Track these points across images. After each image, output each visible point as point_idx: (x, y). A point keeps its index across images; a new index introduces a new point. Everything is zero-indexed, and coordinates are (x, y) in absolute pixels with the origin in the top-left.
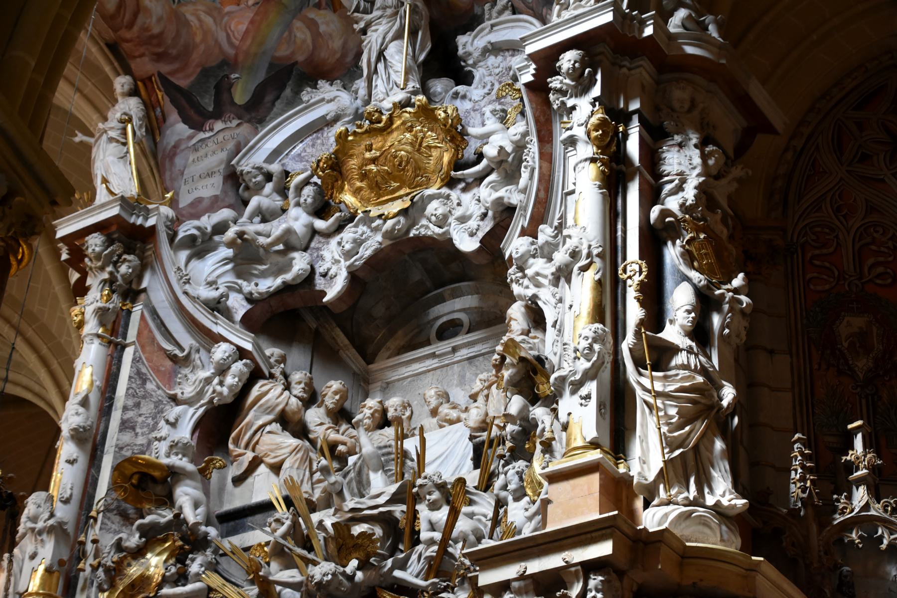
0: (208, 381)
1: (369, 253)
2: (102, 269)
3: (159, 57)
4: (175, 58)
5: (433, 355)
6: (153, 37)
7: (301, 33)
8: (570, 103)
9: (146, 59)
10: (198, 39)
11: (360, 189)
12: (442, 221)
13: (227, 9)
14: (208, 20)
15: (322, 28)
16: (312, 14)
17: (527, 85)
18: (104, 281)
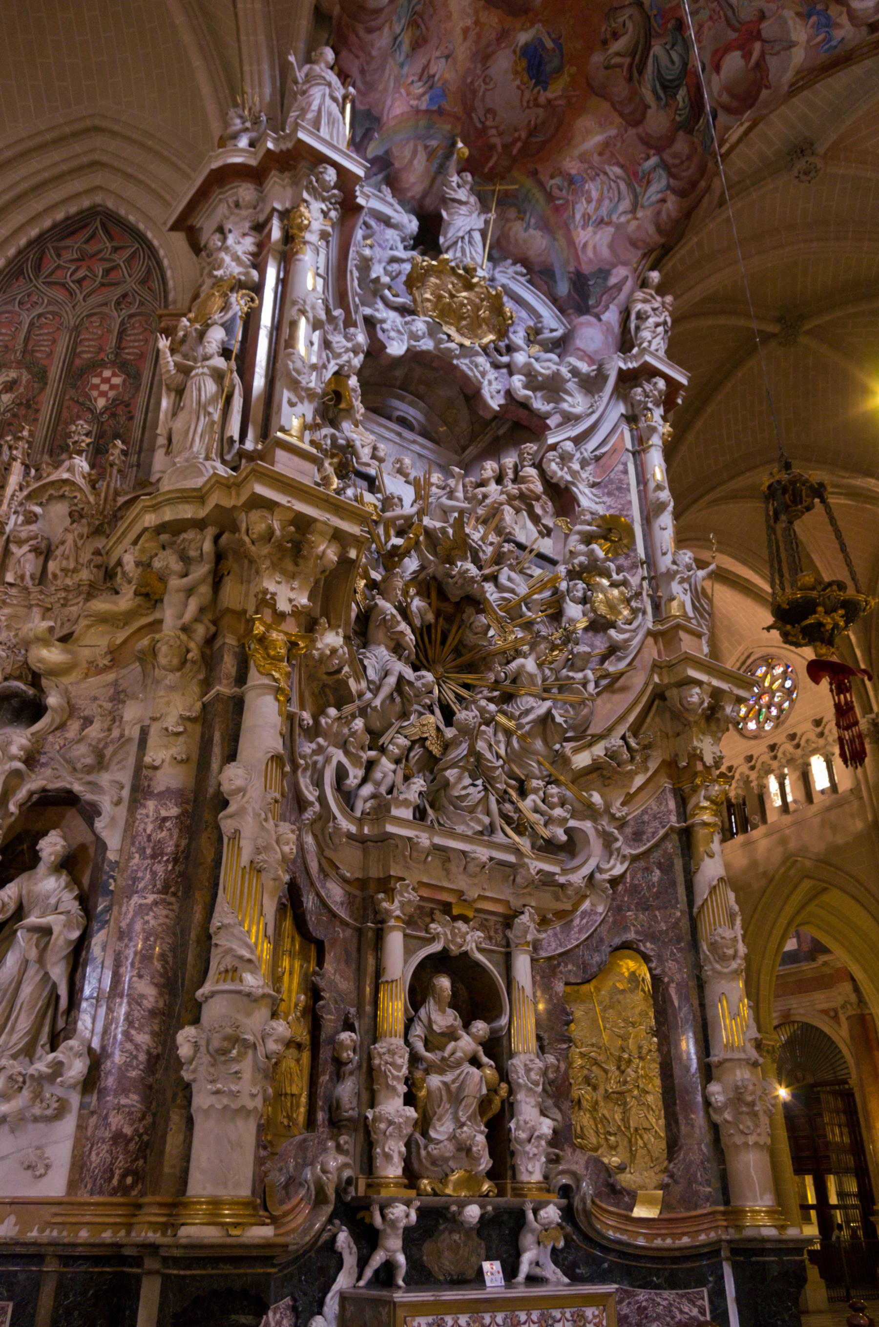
0: (347, 350)
1: (424, 348)
2: (324, 200)
3: (362, 71)
4: (365, 83)
5: (399, 434)
6: (369, 54)
7: (407, 153)
8: (650, 405)
9: (357, 63)
10: (381, 87)
11: (428, 300)
12: (483, 374)
13: (403, 91)
14: (392, 84)
15: (416, 162)
16: (420, 148)
17: (620, 369)
18: (322, 211)
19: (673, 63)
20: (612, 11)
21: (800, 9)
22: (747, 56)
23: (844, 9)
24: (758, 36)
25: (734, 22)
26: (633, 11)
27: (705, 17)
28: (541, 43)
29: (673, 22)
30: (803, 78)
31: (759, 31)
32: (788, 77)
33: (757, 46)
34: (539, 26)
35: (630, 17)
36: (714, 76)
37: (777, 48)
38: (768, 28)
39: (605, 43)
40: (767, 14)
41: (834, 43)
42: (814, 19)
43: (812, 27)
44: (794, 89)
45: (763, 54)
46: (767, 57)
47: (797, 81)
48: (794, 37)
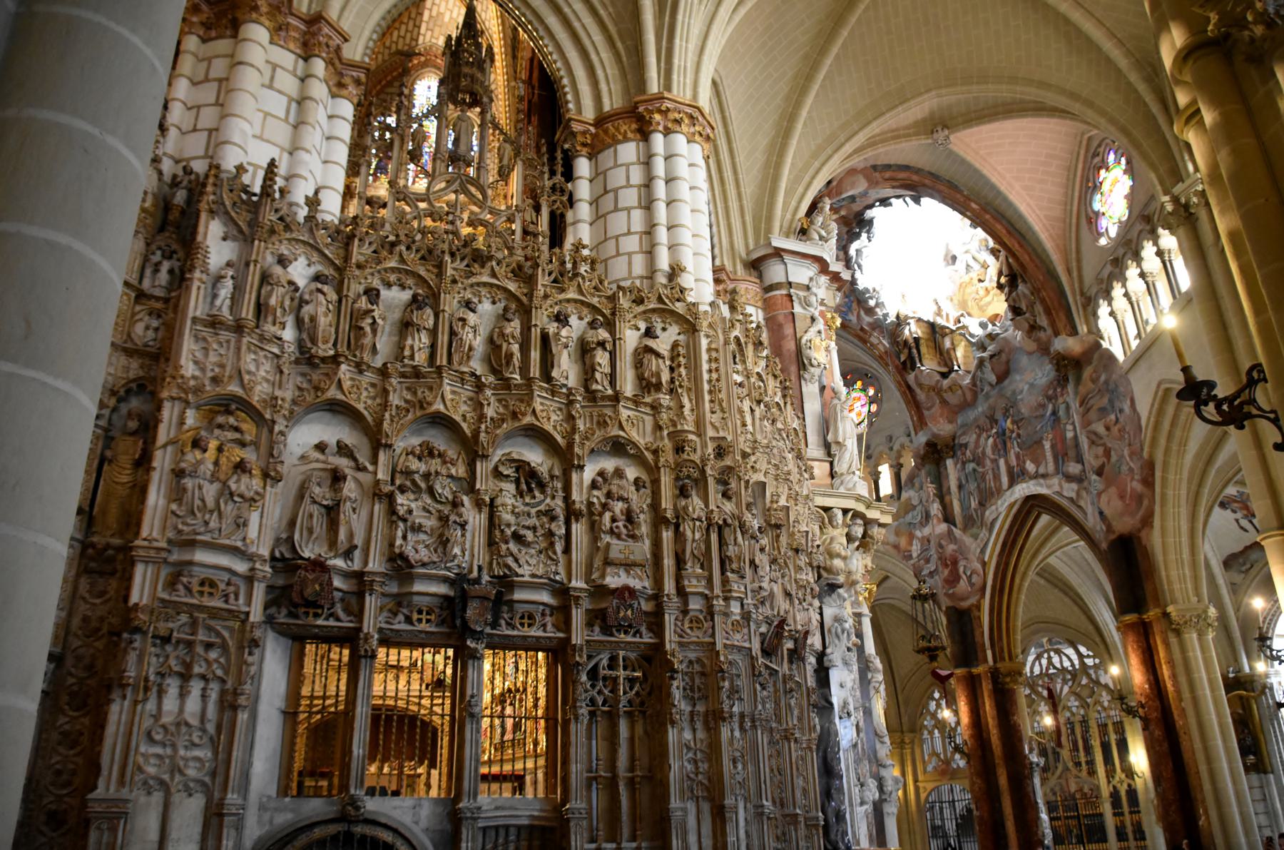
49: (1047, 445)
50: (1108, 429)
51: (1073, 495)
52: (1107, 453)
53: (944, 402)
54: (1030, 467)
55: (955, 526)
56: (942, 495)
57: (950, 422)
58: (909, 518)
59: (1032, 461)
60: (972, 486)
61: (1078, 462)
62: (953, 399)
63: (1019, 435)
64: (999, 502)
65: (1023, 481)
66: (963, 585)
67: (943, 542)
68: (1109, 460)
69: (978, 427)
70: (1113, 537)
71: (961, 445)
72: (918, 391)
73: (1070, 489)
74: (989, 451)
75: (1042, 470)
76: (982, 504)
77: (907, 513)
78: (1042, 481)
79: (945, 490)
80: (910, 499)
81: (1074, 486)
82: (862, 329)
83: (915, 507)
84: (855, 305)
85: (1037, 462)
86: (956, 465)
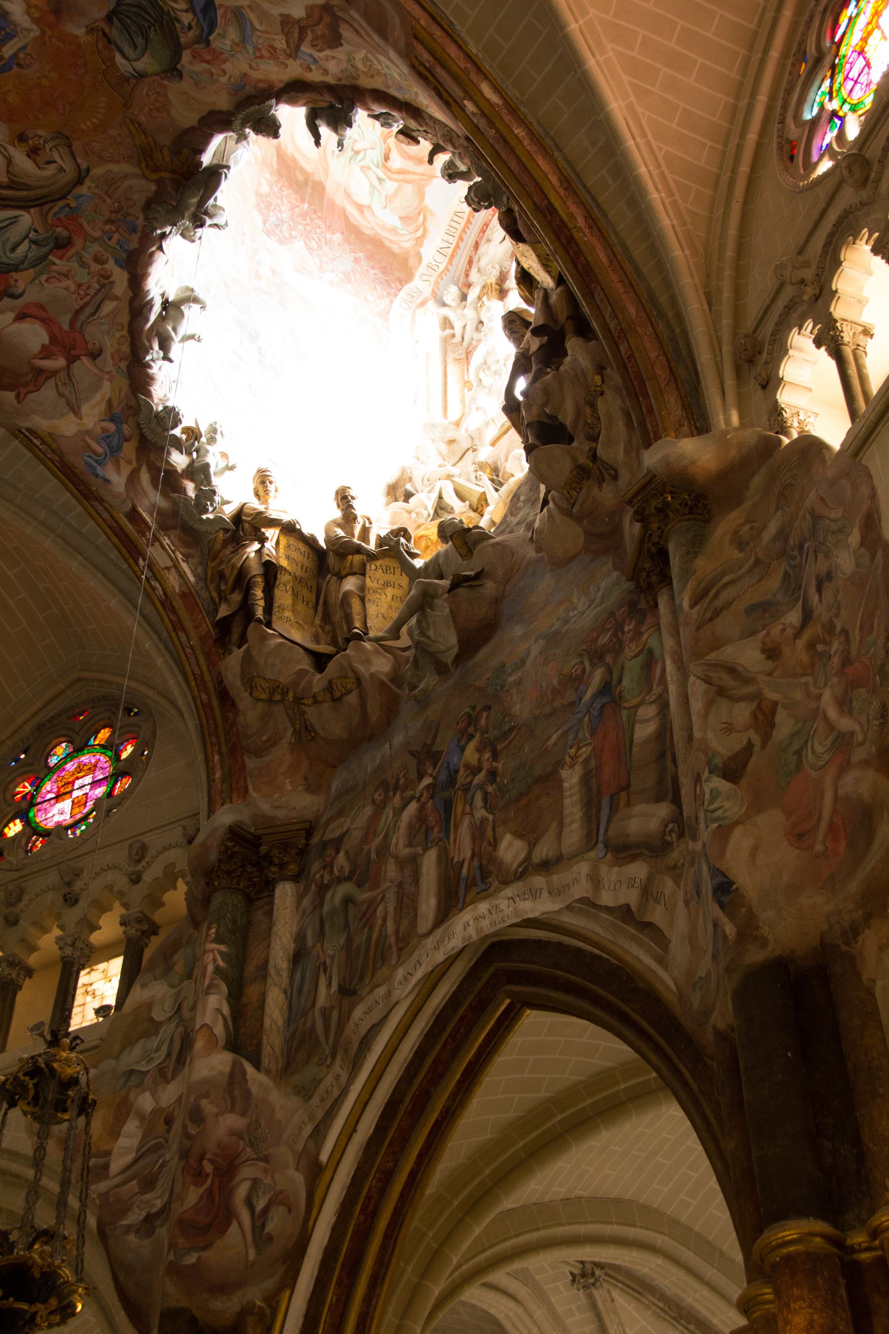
19: (13, 249)
20: (65, 139)
21: (115, 404)
22: (46, 352)
23: (135, 465)
24: (72, 359)
25: (82, 317)
26: (71, 172)
27: (78, 279)
28: (9, 37)
29: (65, 233)
30: (43, 442)
31: (78, 358)
32: (41, 423)
33: (61, 362)
34: (36, 31)
35: (62, 170)
36: (11, 316)
37: (66, 391)
38: (83, 367)
39: (22, 138)
40: (99, 360)
41: (100, 471)
42: (111, 427)
43: (104, 430)
44: (28, 437)
45: (54, 373)
46: (50, 384)
47: (38, 437)
48: (85, 409)
49: (571, 778)
50: (772, 653)
51: (632, 897)
52: (765, 718)
53: (305, 733)
54: (511, 850)
55: (257, 1065)
56: (240, 982)
57: (313, 788)
58: (132, 1058)
59: (518, 835)
60: (332, 948)
61: (659, 799)
62: (331, 723)
63: (493, 775)
64: (400, 973)
65: (485, 894)
66: (235, 1243)
67: (207, 1106)
68: (766, 737)
69: (384, 785)
70: (755, 956)
71: (324, 845)
72: (244, 700)
73: (621, 884)
74: (399, 842)
75: (543, 851)
76: (348, 992)
77: (128, 1043)
78: (538, 881)
79: (251, 967)
80: (149, 1005)
81: (639, 870)
82: (134, 515)
83: (156, 1026)
84: (129, 450)
85: (530, 834)
86: (300, 898)
